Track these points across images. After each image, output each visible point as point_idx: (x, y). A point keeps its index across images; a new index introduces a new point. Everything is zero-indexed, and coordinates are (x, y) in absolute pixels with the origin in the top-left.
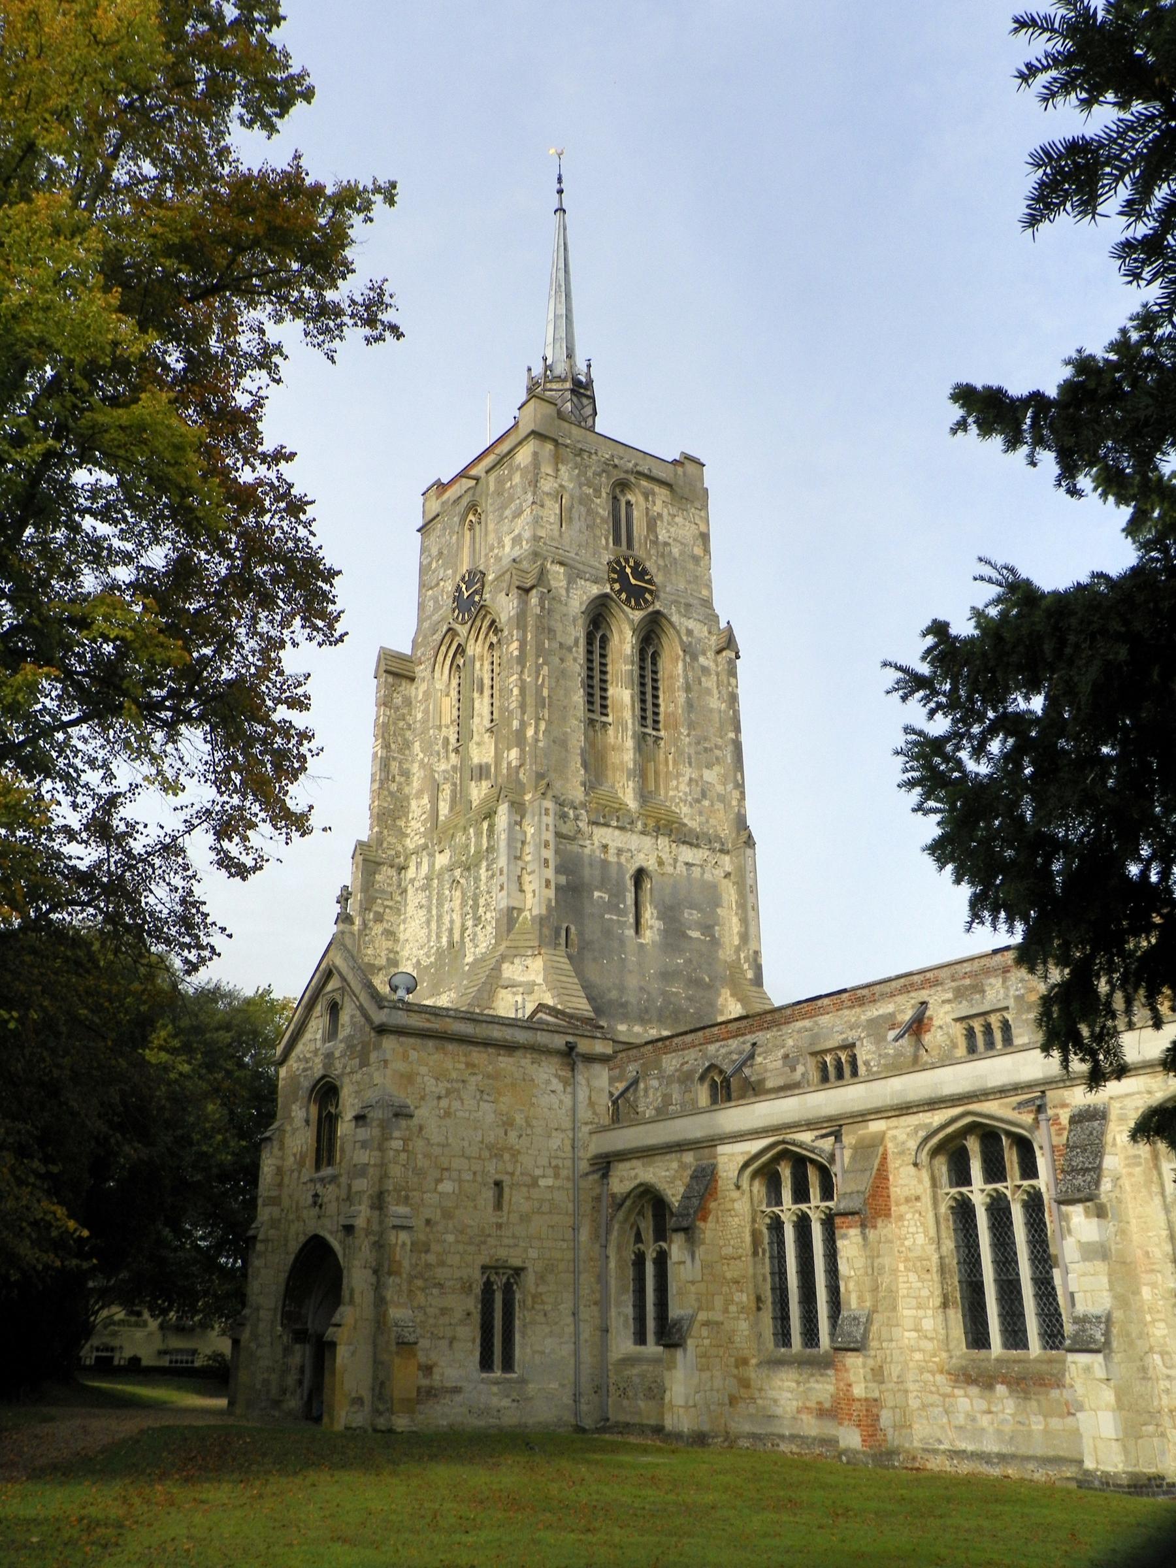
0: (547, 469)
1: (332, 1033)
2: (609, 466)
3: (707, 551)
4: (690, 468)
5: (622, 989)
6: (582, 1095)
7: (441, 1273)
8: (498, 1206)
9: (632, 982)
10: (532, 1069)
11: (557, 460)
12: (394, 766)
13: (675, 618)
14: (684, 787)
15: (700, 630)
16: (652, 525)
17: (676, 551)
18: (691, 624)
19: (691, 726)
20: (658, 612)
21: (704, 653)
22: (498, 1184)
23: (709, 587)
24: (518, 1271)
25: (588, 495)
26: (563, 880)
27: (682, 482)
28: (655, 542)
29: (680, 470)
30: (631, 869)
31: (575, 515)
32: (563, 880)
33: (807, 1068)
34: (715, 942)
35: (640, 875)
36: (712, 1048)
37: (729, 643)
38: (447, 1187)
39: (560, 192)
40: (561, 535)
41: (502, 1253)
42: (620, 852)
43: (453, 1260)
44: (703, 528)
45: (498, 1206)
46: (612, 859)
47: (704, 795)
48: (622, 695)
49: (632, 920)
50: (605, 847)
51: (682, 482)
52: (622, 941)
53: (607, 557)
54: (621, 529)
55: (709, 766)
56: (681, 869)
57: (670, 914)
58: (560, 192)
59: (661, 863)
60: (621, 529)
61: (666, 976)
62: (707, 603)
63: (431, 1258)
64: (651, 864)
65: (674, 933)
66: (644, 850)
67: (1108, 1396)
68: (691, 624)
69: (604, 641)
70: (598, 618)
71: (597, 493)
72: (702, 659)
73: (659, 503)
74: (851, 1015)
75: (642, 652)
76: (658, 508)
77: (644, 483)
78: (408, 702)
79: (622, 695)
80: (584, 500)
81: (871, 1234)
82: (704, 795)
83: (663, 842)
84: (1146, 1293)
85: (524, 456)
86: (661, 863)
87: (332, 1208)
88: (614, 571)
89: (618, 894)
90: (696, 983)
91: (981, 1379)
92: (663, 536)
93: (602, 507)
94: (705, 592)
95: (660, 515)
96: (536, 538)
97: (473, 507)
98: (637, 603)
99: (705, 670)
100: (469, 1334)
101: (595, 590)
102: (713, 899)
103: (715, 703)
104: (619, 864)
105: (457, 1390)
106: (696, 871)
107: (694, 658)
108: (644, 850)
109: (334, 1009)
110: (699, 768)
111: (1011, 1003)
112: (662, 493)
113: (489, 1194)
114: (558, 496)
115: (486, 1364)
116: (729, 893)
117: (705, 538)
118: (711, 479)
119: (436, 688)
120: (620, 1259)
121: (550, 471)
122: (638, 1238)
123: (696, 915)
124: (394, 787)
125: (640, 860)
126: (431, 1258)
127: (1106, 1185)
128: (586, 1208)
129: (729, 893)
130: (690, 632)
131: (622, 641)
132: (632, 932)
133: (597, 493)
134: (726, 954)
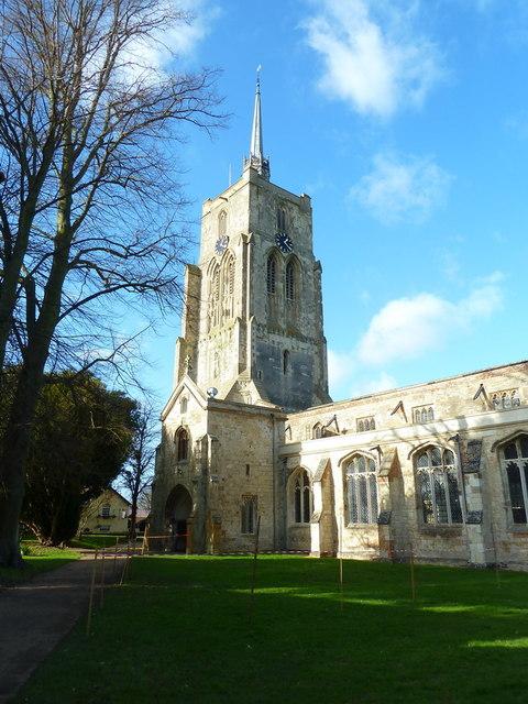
1: (184, 409)
2: (275, 197)
6: (276, 433)
7: (228, 498)
8: (247, 473)
10: (259, 424)
15: (308, 262)
22: (248, 466)
24: (255, 497)
26: (258, 354)
27: (304, 205)
32: (258, 354)
33: (354, 426)
35: (286, 352)
36: (318, 416)
37: (318, 266)
38: (229, 466)
41: (250, 490)
42: (279, 343)
43: (232, 493)
45: (247, 473)
48: (280, 285)
51: (304, 205)
52: (279, 376)
53: (275, 232)
54: (281, 223)
57: (296, 367)
60: (281, 223)
61: (295, 390)
63: (225, 492)
65: (297, 373)
66: (287, 343)
67: (480, 538)
74: (375, 405)
76: (293, 215)
79: (280, 285)
80: (268, 210)
84: (493, 504)
87: (186, 475)
90: (304, 392)
91: (431, 533)
92: (296, 224)
100: (238, 519)
101: (271, 245)
102: (312, 363)
103: (313, 289)
105: (234, 539)
108: (287, 343)
109: (185, 401)
111: (434, 401)
112: (296, 209)
113: (245, 469)
115: (243, 531)
116: (317, 360)
117: (311, 226)
118: (313, 204)
120: (291, 492)
122: (298, 484)
126: (225, 492)
127: (481, 467)
128: (276, 474)
129: (317, 360)
134: (315, 382)
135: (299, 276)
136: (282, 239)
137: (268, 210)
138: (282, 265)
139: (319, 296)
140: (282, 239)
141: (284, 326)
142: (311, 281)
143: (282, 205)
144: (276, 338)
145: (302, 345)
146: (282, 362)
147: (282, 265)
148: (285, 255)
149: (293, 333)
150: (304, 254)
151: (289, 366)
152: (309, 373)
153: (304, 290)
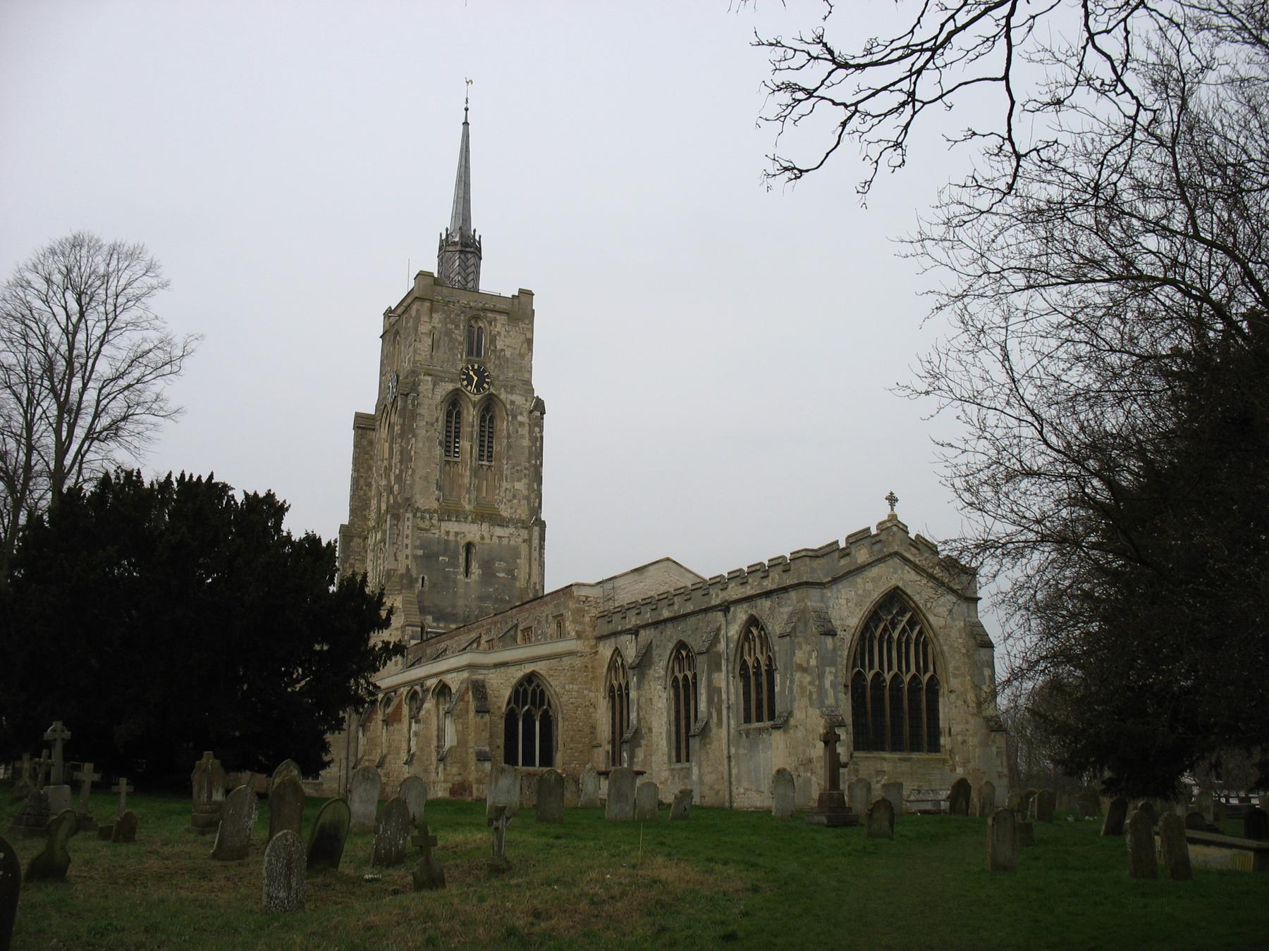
0: (425, 318)
3: (530, 349)
4: (523, 299)
5: (454, 606)
9: (460, 603)
11: (432, 310)
12: (362, 482)
13: (503, 396)
14: (502, 494)
15: (518, 399)
16: (493, 341)
17: (508, 354)
18: (514, 397)
19: (509, 458)
20: (492, 394)
21: (521, 414)
23: (531, 372)
25: (451, 330)
27: (519, 309)
28: (494, 351)
29: (516, 301)
30: (463, 542)
31: (442, 343)
34: (514, 578)
35: (469, 547)
37: (540, 406)
39: (467, 109)
40: (431, 357)
42: (457, 534)
44: (529, 336)
46: (452, 538)
47: (514, 497)
49: (462, 569)
50: (448, 533)
51: (519, 309)
52: (455, 582)
53: (461, 365)
54: (474, 347)
55: (519, 480)
56: (495, 540)
58: (467, 109)
59: (482, 538)
60: (474, 347)
61: (482, 598)
64: (477, 539)
66: (473, 532)
68: (514, 397)
69: (459, 414)
70: (454, 403)
71: (457, 327)
72: (519, 418)
73: (499, 325)
75: (483, 419)
77: (489, 315)
78: (371, 443)
81: (391, 728)
82: (514, 497)
83: (485, 526)
86: (482, 538)
88: (464, 374)
89: (454, 557)
93: (460, 335)
94: (526, 376)
95: (499, 333)
96: (415, 362)
97: (397, 332)
98: (478, 391)
99: (521, 424)
101: (450, 387)
104: (456, 542)
106: (505, 541)
107: (514, 417)
108: (473, 532)
110: (513, 481)
112: (502, 319)
114: (431, 334)
116: (524, 549)
121: (427, 319)
123: (503, 564)
124: (362, 493)
125: (469, 538)
130: (512, 403)
131: (468, 413)
132: (461, 577)
133: (457, 327)
135: (502, 426)
137: (449, 333)
138: (471, 415)
139: (537, 453)
141: (468, 507)
142: (524, 431)
143: (477, 318)
144: (453, 527)
145: (499, 531)
147: (471, 415)
149: (488, 516)
150: (511, 389)
151: (475, 567)
152: (510, 572)
153: (509, 446)
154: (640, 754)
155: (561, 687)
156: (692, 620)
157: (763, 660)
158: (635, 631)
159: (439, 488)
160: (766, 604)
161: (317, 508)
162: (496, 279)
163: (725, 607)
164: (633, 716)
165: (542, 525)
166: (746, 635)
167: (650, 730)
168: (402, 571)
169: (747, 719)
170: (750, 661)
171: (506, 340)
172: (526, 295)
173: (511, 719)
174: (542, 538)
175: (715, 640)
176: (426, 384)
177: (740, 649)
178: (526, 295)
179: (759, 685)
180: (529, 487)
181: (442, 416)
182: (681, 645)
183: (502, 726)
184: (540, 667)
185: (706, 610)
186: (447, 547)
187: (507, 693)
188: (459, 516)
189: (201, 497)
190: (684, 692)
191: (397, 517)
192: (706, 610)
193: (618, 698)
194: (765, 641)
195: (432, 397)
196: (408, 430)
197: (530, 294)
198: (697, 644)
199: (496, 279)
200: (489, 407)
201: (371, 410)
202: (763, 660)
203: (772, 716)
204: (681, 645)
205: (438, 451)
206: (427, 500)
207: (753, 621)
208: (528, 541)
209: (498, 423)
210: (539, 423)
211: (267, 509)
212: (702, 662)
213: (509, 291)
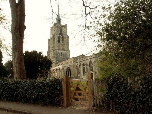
15: (66, 36)
16: (63, 30)
27: (66, 26)
35: (61, 53)
37: (68, 37)
48: (61, 42)
51: (66, 26)
61: (63, 59)
62: (67, 34)
65: (64, 56)
70: (59, 37)
79: (61, 42)
83: (63, 51)
85: (54, 27)
89: (60, 54)
99: (66, 39)
101: (58, 35)
108: (62, 51)
112: (64, 27)
117: (67, 30)
118: (68, 26)
119: (51, 41)
135: (64, 39)
136: (61, 34)
138: (61, 39)
139: (68, 42)
140: (61, 34)
141: (61, 49)
142: (67, 40)
145: (64, 51)
146: (61, 54)
147: (61, 39)
148: (61, 36)
149: (63, 49)
151: (62, 55)
154: (80, 75)
155: (72, 69)
156: (85, 61)
157: (91, 65)
158: (79, 62)
159: (58, 47)
160: (92, 59)
161: (45, 54)
162: (62, 23)
163: (88, 60)
164: (79, 71)
165: (69, 50)
166: (90, 62)
167: (81, 72)
168: (54, 56)
169: (90, 71)
170: (90, 65)
171: (64, 29)
172: (66, 24)
173: (67, 72)
174: (69, 52)
175: (87, 63)
176: (56, 35)
177: (89, 64)
178: (66, 24)
179: (91, 68)
180: (68, 46)
181: (57, 38)
182: (84, 64)
183: (66, 73)
184: (69, 66)
185: (86, 60)
186: (59, 53)
187: (66, 69)
188: (60, 50)
189: (34, 53)
190: (84, 68)
191: (53, 50)
192: (86, 60)
193: (77, 69)
194: (92, 63)
195: (56, 37)
196: (54, 40)
197: (67, 24)
198: (85, 63)
199: (62, 23)
200: (63, 38)
201: (50, 38)
202: (91, 65)
203: (92, 70)
204: (84, 64)
205: (57, 43)
206: (57, 48)
207: (90, 61)
208: (68, 52)
209: (64, 39)
210: (68, 39)
211: (40, 53)
212: (86, 65)
213: (64, 24)
